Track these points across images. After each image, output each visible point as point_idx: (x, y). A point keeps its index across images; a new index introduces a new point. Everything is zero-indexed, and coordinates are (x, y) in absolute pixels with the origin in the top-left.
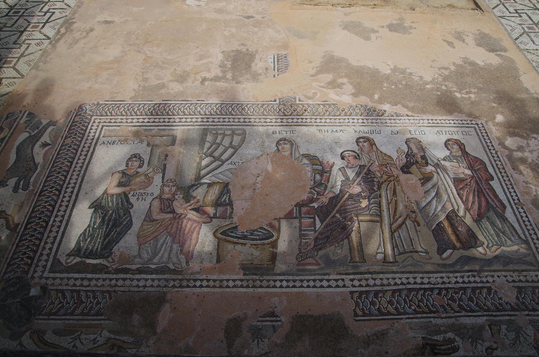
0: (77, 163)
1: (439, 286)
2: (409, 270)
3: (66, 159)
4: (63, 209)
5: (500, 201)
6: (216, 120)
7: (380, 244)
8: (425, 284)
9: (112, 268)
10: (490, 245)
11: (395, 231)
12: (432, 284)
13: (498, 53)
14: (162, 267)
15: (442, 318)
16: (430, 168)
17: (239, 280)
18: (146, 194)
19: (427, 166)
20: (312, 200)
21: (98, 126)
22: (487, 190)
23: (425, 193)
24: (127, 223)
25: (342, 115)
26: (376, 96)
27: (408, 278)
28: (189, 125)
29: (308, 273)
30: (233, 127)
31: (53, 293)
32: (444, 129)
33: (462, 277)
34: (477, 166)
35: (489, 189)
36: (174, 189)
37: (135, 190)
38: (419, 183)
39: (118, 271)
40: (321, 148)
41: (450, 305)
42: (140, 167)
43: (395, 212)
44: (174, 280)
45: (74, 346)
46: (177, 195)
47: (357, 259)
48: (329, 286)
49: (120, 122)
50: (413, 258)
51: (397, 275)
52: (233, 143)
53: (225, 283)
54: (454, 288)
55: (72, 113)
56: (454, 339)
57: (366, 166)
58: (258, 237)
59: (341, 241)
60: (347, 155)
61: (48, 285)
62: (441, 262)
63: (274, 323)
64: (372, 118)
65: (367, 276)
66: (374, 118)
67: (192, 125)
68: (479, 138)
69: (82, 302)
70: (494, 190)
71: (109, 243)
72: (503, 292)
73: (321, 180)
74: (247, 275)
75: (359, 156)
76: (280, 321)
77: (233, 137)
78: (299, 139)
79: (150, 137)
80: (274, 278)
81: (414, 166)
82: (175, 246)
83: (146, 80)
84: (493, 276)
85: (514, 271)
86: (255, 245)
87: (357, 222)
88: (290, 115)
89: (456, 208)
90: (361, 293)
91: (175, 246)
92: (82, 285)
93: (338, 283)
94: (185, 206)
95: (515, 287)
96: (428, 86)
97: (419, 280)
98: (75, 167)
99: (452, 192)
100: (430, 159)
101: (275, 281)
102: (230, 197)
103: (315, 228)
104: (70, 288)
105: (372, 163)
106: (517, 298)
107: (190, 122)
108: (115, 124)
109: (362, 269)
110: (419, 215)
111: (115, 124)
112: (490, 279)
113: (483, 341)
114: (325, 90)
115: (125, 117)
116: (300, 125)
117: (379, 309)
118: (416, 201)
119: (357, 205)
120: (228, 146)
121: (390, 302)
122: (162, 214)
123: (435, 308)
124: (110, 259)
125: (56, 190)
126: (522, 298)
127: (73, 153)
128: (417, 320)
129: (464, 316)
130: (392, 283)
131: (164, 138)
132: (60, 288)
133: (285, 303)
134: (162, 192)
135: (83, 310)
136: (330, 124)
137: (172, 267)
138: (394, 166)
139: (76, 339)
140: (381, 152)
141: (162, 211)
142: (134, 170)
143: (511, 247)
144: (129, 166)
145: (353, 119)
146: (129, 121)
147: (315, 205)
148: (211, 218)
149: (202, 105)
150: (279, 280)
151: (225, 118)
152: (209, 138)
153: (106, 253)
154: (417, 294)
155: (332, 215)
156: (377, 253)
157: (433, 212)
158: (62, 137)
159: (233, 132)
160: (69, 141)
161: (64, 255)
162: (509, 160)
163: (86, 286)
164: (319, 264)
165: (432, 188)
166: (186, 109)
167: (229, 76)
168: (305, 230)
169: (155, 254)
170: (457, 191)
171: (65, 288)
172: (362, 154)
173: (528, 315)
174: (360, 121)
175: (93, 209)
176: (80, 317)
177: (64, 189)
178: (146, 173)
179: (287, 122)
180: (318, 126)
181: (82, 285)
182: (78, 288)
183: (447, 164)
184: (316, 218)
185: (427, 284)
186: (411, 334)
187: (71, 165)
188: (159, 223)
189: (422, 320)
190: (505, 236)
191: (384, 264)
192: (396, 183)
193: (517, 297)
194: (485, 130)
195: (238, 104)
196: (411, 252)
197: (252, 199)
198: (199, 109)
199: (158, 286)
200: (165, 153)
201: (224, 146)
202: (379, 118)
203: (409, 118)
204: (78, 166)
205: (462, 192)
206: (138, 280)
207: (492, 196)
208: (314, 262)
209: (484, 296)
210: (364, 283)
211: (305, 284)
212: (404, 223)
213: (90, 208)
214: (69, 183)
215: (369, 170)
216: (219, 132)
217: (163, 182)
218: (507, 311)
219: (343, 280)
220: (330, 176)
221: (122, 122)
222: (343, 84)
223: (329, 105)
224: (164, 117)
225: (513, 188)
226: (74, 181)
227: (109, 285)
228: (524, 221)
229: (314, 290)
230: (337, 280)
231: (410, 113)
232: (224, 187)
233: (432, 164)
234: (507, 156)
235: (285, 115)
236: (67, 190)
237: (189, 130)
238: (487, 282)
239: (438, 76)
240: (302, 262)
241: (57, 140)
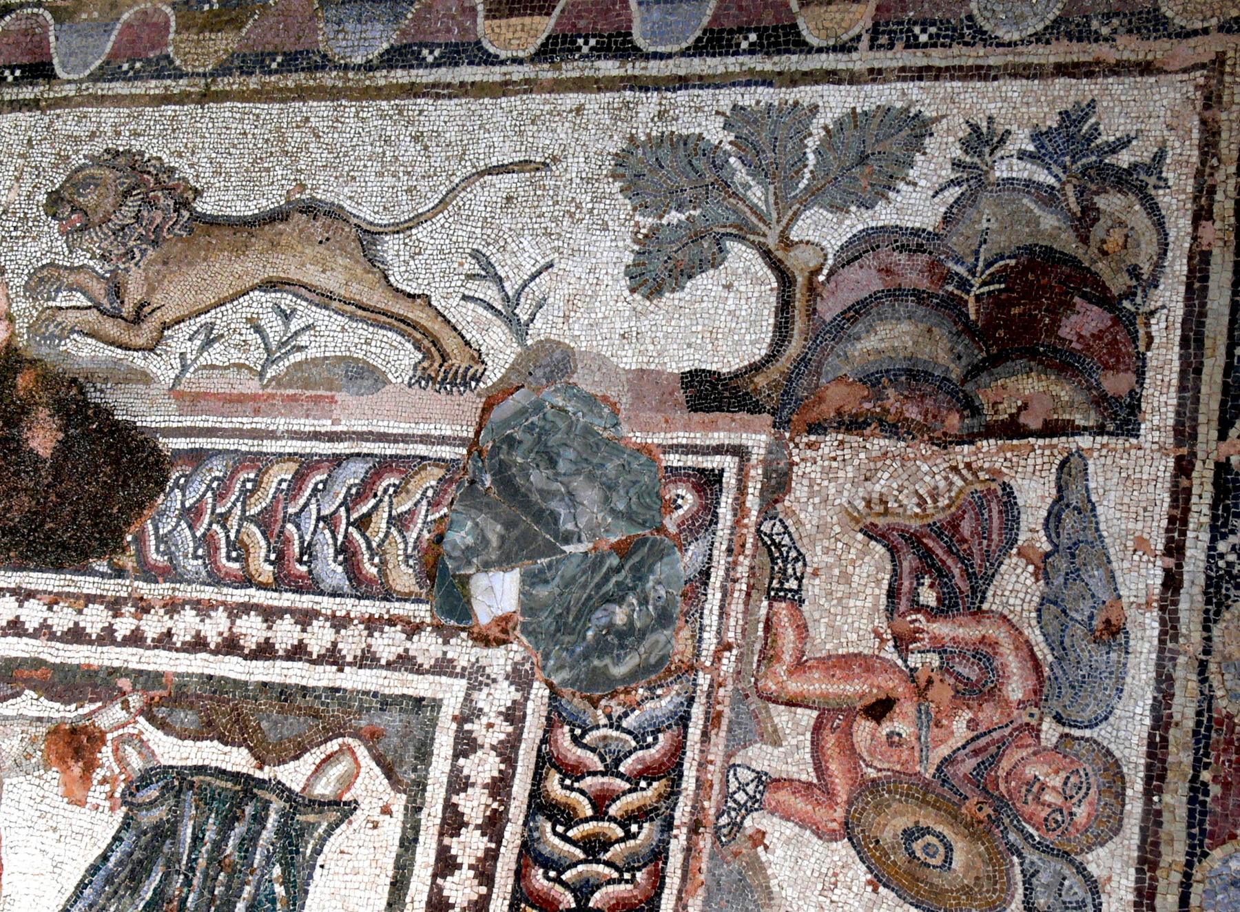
9: (126, 706)
31: (404, 578)
45: (287, 317)
61: (438, 628)
69: (265, 522)
71: (137, 873)
92: (270, 615)
124: (136, 763)
135: (257, 483)
139: (282, 344)
163: (246, 608)
181: (270, 615)
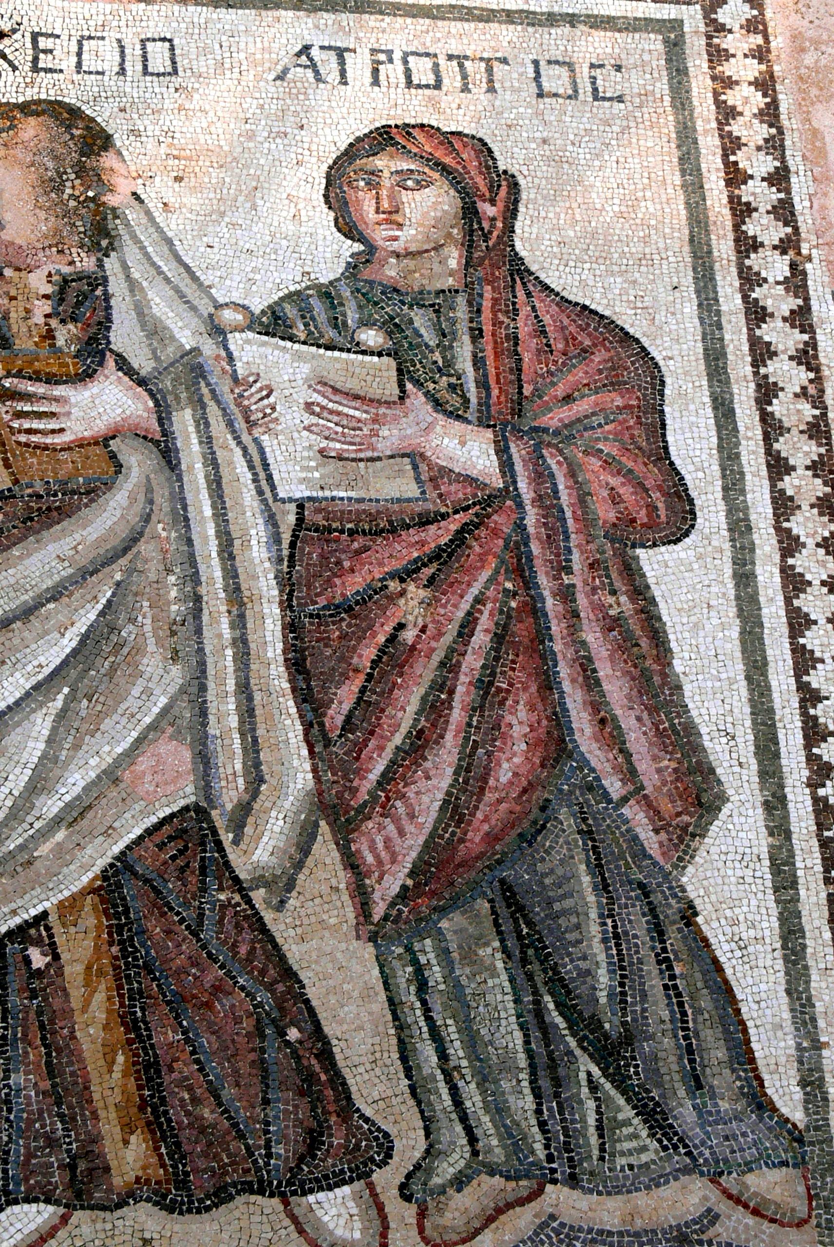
5: (679, 738)
10: (446, 1170)
16: (103, 403)
19: (86, 376)
22: (592, 635)
34: (573, 400)
35: (612, 624)
68: (686, 137)
89: (230, 792)
99: (241, 645)
100: (141, 311)
143: (641, 1199)
165: (56, 594)
170: (291, 627)
183: (284, 368)
190: (621, 1083)
194: (761, 54)
233: (143, 363)
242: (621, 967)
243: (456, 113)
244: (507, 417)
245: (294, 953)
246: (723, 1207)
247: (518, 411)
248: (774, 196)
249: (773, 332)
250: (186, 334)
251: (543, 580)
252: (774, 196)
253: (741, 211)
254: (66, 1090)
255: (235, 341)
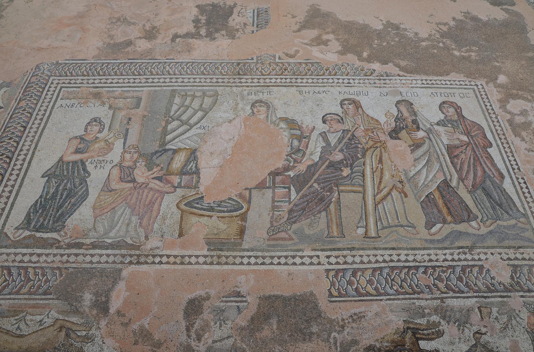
0: (31, 128)
1: (425, 264)
2: (393, 247)
3: (19, 123)
4: (13, 178)
5: (498, 170)
6: (186, 80)
7: (361, 217)
8: (409, 262)
10: (485, 219)
11: (379, 203)
12: (417, 261)
13: (504, 7)
14: (119, 242)
15: (426, 300)
16: (421, 134)
17: (202, 256)
18: (105, 161)
19: (418, 131)
20: (287, 169)
21: (56, 87)
22: (485, 159)
23: (415, 161)
24: (83, 193)
25: (326, 74)
26: (365, 54)
27: (390, 255)
28: (155, 86)
29: (280, 248)
30: (204, 88)
32: (439, 91)
33: (452, 254)
36: (136, 156)
37: (92, 157)
38: (409, 150)
39: (70, 246)
40: (300, 111)
41: (436, 285)
42: (100, 132)
43: (380, 182)
44: (131, 256)
45: (18, 328)
46: (139, 162)
47: (335, 234)
48: (303, 264)
49: (80, 83)
50: (398, 233)
51: (379, 251)
52: (204, 106)
53: (187, 259)
54: (442, 266)
55: (28, 73)
56: (439, 322)
57: (350, 131)
58: (226, 209)
59: (318, 213)
60: (330, 118)
62: (429, 237)
63: (238, 304)
64: (359, 78)
65: (345, 253)
66: (361, 78)
67: (159, 86)
69: (29, 280)
70: (492, 159)
71: (62, 214)
72: (497, 270)
73: (299, 147)
74: (212, 250)
75: (342, 119)
76: (245, 301)
77: (204, 98)
78: (276, 101)
79: (113, 99)
80: (241, 254)
81: (404, 131)
82: (134, 219)
83: (111, 37)
84: (486, 254)
85: (509, 247)
86: (222, 217)
87: (337, 193)
88: (267, 75)
89: (449, 178)
90: (338, 271)
91: (134, 219)
93: (313, 260)
94: (147, 174)
95: (511, 265)
96: (424, 44)
97: (403, 258)
98: (29, 132)
101: (242, 257)
102: (197, 164)
103: (290, 199)
104: (16, 264)
105: (357, 128)
106: (512, 278)
107: (158, 82)
108: (75, 85)
109: (340, 245)
110: (407, 185)
111: (75, 85)
112: (483, 257)
113: (471, 325)
114: (309, 47)
115: (87, 78)
116: (279, 86)
117: (356, 290)
118: (404, 170)
119: (338, 173)
120: (197, 108)
121: (370, 282)
122: (122, 183)
123: (419, 288)
124: (62, 233)
125: (7, 157)
126: (517, 278)
127: (27, 117)
128: (399, 302)
129: (452, 297)
130: (373, 260)
131: (128, 100)
132: (6, 264)
133: (252, 282)
134: (123, 158)
135: (31, 288)
136: (312, 85)
137: (130, 241)
138: (381, 131)
139: (21, 321)
140: (368, 115)
141: (121, 180)
142: (93, 136)
143: (508, 222)
144: (88, 130)
145: (338, 79)
146: (90, 82)
147: (291, 174)
148: (175, 188)
149: (172, 64)
150: (247, 257)
151: (196, 78)
152: (177, 100)
153: (58, 226)
154: (400, 272)
155: (309, 185)
156: (358, 227)
157: (422, 182)
158: (16, 100)
159: (204, 93)
160: (23, 104)
161: (13, 228)
162: (510, 125)
164: (293, 239)
165: (422, 156)
166: (154, 68)
167: (203, 32)
168: (278, 202)
169: (112, 228)
170: (450, 158)
171: (11, 265)
172: (346, 118)
173: (522, 296)
174: (346, 81)
175: (47, 178)
176: (27, 297)
177: (15, 156)
178: (107, 138)
179: (264, 83)
180: (298, 86)
181: (30, 261)
182: (25, 265)
183: (440, 129)
184: (292, 188)
185: (412, 262)
186: (392, 317)
187: (25, 130)
188: (118, 193)
189: (404, 301)
190: (501, 208)
191: (366, 239)
192: (383, 150)
193: (512, 276)
194: (485, 91)
195: (211, 63)
196: (396, 226)
197: (221, 167)
198: (168, 68)
199: (114, 262)
200: (128, 116)
201: (193, 109)
202: (366, 77)
203: (401, 78)
204: (32, 131)
205: (456, 160)
206: (92, 256)
207: (489, 165)
208: (287, 236)
209: (475, 275)
210: (341, 260)
211: (276, 261)
212: (389, 193)
213: (43, 177)
214: (21, 150)
215: (353, 135)
216: (189, 93)
217: (124, 148)
218: (499, 292)
219: (318, 257)
220: (309, 142)
221: (82, 83)
222: (328, 41)
223: (312, 64)
224: (129, 77)
225: (513, 156)
226: (27, 147)
227: (60, 261)
228: (524, 193)
229: (285, 267)
230: (311, 257)
231: (401, 73)
232: (191, 154)
234: (508, 121)
235: (263, 75)
236: (19, 158)
237: (155, 91)
238: (480, 260)
239: (435, 32)
240: (274, 237)
241: (10, 103)
242: (498, 196)
243: (451, 99)
244: (467, 133)
245: (461, 195)
246: (518, 223)
247: (469, 133)
248: (491, 108)
249: (495, 123)
250: (429, 126)
251: (477, 152)
252: (491, 108)
253: (488, 110)
254: (440, 211)
255: (434, 126)
